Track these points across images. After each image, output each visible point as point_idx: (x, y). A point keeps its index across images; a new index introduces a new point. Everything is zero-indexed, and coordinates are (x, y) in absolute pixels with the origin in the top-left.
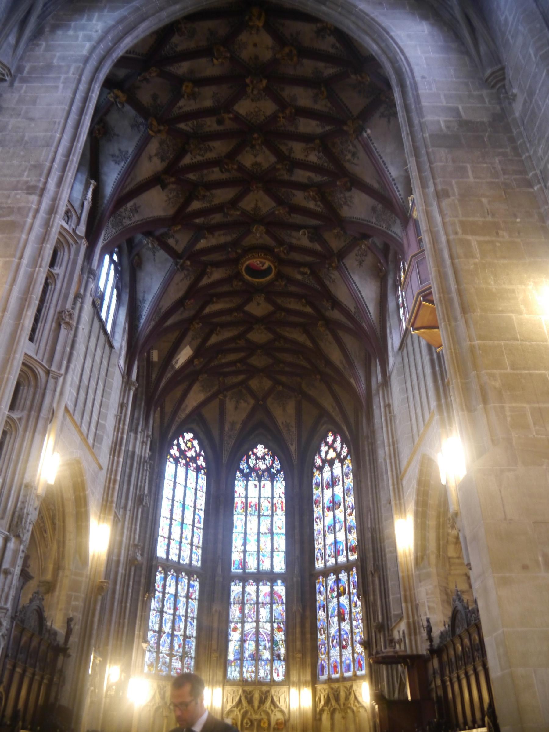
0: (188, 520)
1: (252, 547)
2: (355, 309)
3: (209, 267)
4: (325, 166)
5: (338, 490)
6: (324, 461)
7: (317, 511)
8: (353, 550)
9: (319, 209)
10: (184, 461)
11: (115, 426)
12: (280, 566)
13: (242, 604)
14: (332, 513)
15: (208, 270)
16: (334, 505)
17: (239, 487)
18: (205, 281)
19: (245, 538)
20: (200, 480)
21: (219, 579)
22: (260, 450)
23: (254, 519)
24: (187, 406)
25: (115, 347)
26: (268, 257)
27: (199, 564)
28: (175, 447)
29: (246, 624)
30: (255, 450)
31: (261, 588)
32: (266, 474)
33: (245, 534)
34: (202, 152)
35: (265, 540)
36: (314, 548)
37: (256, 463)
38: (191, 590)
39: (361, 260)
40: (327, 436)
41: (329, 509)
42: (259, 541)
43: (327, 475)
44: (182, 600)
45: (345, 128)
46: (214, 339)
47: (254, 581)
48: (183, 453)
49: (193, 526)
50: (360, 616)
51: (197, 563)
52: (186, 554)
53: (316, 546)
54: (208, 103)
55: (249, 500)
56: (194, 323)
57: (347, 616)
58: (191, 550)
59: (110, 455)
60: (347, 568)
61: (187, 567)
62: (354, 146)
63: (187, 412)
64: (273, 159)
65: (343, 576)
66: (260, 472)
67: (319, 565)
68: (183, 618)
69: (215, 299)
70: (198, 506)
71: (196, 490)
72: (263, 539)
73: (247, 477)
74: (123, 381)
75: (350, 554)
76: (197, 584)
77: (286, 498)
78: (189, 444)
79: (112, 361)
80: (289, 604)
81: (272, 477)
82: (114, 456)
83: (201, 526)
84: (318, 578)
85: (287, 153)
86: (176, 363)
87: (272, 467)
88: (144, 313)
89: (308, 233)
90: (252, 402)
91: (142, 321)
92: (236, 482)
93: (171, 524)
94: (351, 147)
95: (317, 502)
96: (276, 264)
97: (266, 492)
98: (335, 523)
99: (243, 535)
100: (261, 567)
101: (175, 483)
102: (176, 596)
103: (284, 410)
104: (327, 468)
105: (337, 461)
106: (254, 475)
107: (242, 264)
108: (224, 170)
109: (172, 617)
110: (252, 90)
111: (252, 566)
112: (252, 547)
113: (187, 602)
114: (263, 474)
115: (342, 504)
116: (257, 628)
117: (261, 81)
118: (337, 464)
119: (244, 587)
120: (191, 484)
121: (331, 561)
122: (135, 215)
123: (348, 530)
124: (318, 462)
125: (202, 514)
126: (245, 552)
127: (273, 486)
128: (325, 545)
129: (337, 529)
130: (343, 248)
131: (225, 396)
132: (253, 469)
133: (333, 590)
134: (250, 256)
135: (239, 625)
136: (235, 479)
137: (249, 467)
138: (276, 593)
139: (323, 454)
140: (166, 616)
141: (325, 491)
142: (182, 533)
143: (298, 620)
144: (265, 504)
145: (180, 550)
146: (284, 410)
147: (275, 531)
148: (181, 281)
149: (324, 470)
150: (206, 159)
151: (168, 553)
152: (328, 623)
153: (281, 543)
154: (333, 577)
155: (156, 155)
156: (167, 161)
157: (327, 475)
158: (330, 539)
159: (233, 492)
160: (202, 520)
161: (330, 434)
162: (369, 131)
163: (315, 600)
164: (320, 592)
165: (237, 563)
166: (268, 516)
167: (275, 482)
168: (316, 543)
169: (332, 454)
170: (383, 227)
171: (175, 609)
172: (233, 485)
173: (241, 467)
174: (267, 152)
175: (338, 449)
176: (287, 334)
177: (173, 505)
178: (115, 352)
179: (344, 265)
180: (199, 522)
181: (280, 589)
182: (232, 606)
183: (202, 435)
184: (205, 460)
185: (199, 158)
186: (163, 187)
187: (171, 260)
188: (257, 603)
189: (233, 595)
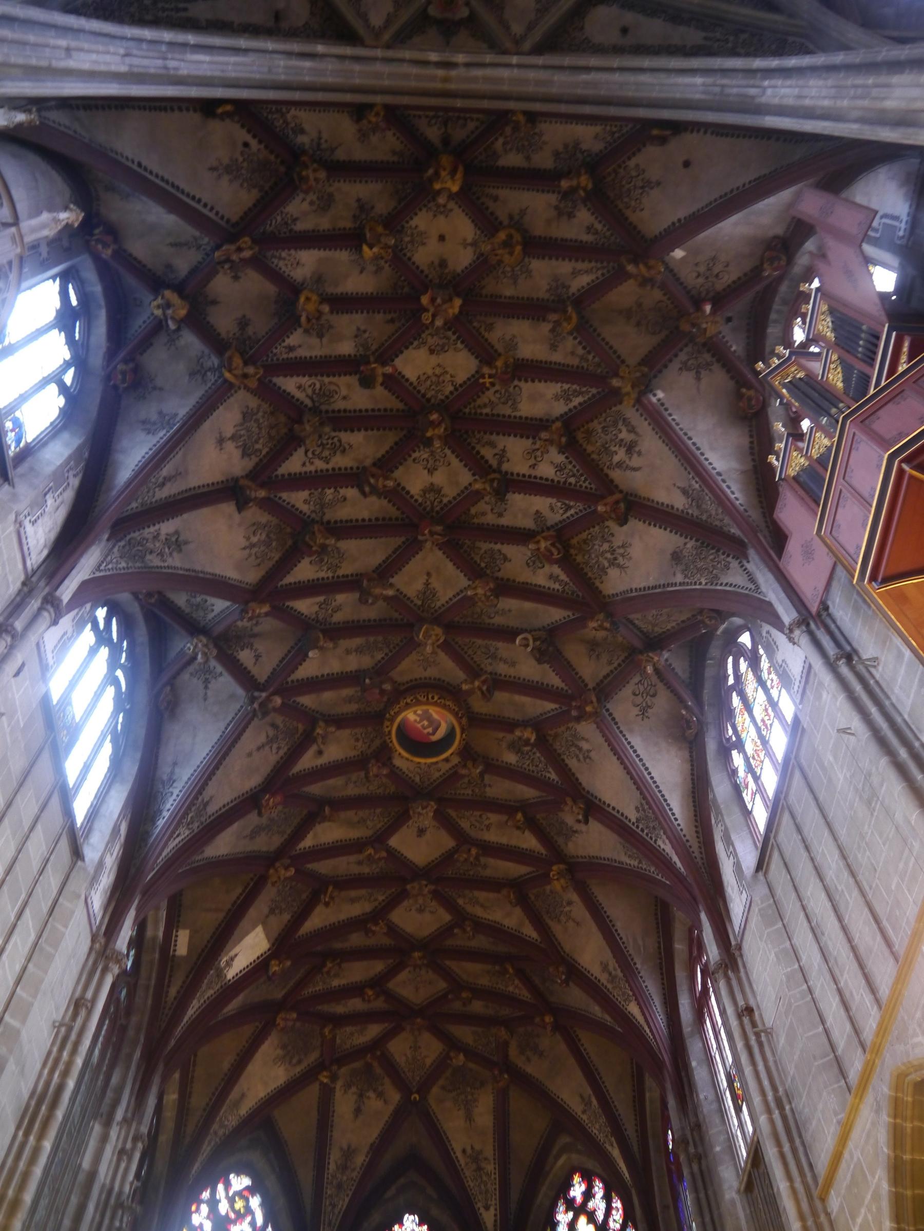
2: (638, 811)
3: (321, 724)
4: (570, 484)
9: (557, 586)
11: (49, 1053)
15: (319, 731)
18: (308, 761)
24: (243, 1096)
25: (86, 859)
26: (448, 703)
28: (204, 1208)
34: (326, 453)
39: (644, 705)
40: (569, 1185)
45: (615, 382)
46: (318, 920)
54: (346, 348)
56: (277, 864)
59: (18, 1128)
62: (632, 430)
63: (244, 1110)
64: (465, 477)
69: (327, 809)
74: (91, 949)
78: (239, 1205)
79: (71, 887)
82: (27, 1134)
85: (494, 463)
86: (229, 964)
88: (168, 806)
89: (535, 640)
90: (395, 1097)
91: (161, 823)
94: (624, 435)
96: (464, 721)
103: (469, 1118)
107: (392, 720)
108: (367, 489)
110: (434, 316)
117: (451, 300)
122: (175, 554)
130: (605, 677)
131: (334, 1078)
134: (409, 701)
146: (469, 1118)
148: (259, 749)
150: (333, 469)
155: (233, 438)
156: (255, 460)
161: (577, 1179)
162: (660, 394)
170: (700, 584)
174: (455, 462)
175: (600, 1216)
176: (479, 912)
178: (85, 869)
179: (610, 715)
183: (272, 1182)
185: (319, 465)
186: (240, 508)
187: (240, 692)
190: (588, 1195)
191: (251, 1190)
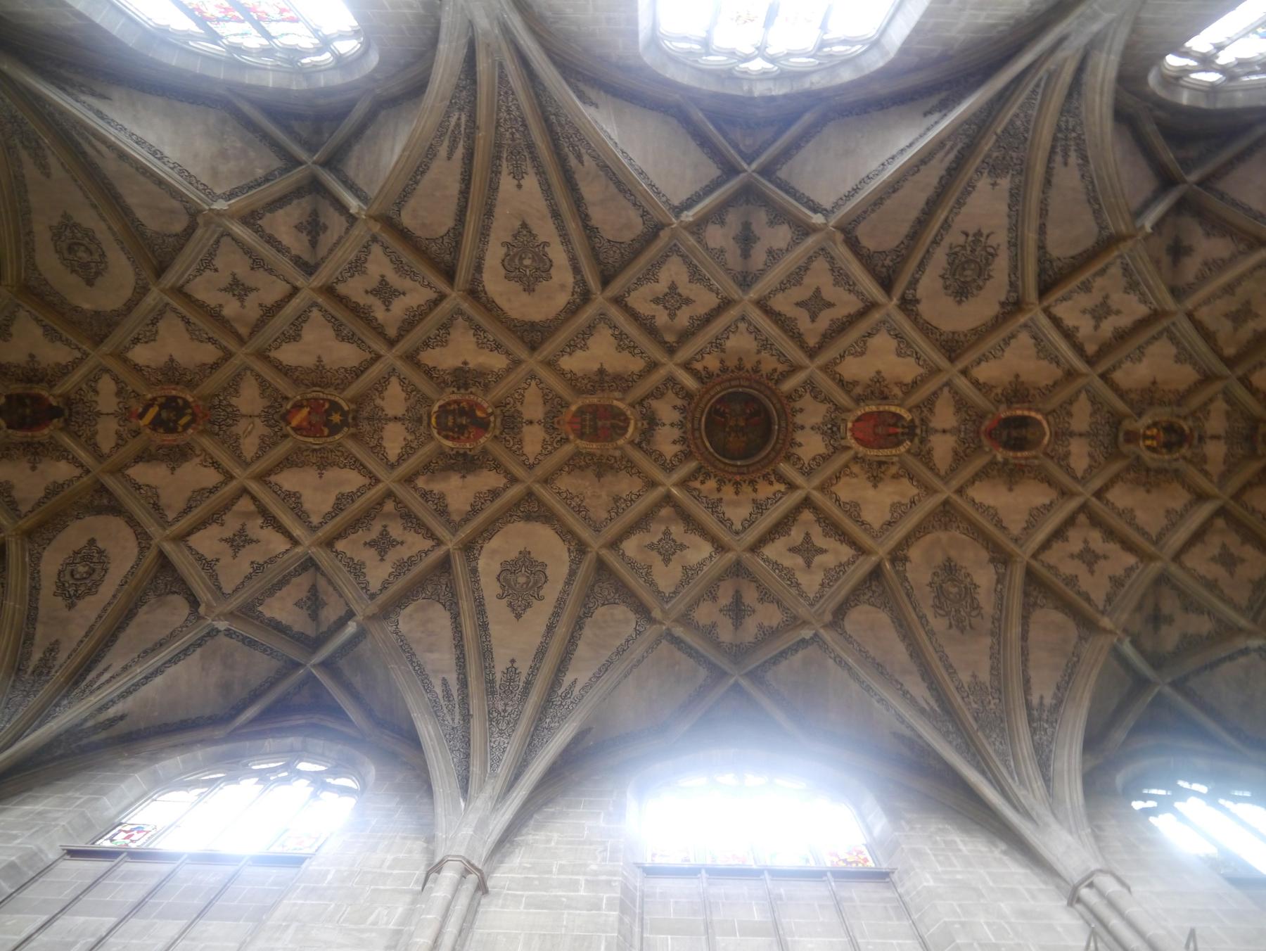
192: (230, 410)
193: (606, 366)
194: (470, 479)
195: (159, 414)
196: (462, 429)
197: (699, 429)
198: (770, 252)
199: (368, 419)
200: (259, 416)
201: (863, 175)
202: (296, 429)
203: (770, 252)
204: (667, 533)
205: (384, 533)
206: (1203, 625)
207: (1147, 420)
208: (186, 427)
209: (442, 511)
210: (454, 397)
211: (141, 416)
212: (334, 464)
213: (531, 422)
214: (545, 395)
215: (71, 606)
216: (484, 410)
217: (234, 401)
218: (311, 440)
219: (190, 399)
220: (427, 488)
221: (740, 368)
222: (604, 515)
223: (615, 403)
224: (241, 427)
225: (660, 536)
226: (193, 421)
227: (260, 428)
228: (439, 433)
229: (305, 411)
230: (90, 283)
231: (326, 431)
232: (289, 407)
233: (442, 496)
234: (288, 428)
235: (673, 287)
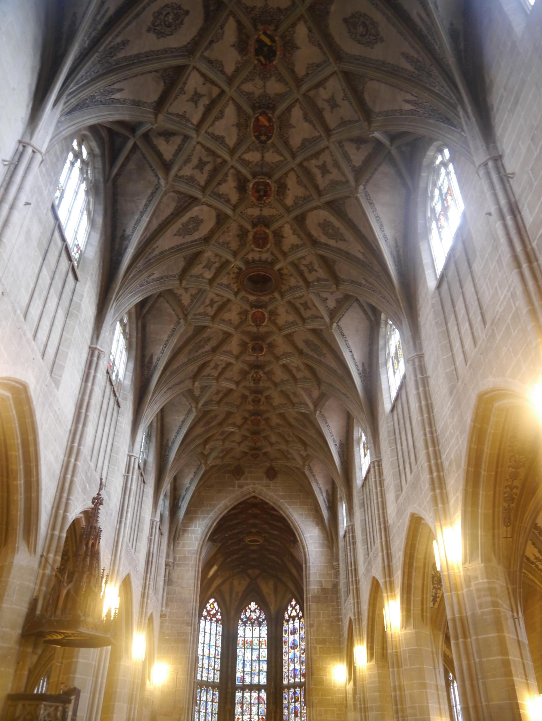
0: (212, 655)
1: (248, 669)
5: (297, 637)
6: (290, 616)
7: (285, 648)
8: (303, 675)
10: (209, 618)
12: (263, 681)
13: (242, 704)
14: (293, 651)
16: (294, 647)
17: (240, 632)
19: (244, 663)
20: (218, 629)
21: (230, 690)
22: (253, 606)
23: (249, 651)
27: (218, 681)
29: (244, 716)
30: (250, 606)
31: (252, 694)
32: (256, 622)
33: (244, 660)
35: (255, 664)
36: (283, 671)
37: (250, 615)
38: (214, 697)
40: (291, 601)
41: (291, 647)
42: (251, 665)
43: (291, 626)
44: (210, 703)
47: (249, 690)
48: (208, 612)
49: (215, 657)
50: (305, 715)
51: (217, 681)
52: (211, 676)
53: (284, 670)
55: (246, 639)
57: (299, 714)
58: (214, 672)
60: (301, 685)
61: (212, 684)
65: (298, 690)
66: (253, 621)
67: (285, 682)
68: (210, 714)
70: (218, 645)
71: (216, 634)
72: (254, 664)
73: (245, 623)
75: (302, 678)
76: (217, 693)
77: (267, 638)
78: (212, 606)
80: (268, 704)
81: (260, 624)
83: (219, 657)
84: (284, 690)
87: (259, 617)
90: (248, 580)
92: (239, 627)
93: (203, 659)
95: (285, 642)
97: (256, 634)
98: (294, 657)
99: (242, 661)
100: (253, 682)
101: (205, 632)
102: (206, 702)
104: (291, 622)
105: (297, 618)
106: (249, 622)
109: (204, 714)
111: (248, 680)
112: (248, 669)
113: (212, 704)
114: (254, 622)
115: (299, 647)
116: (250, 718)
118: (297, 621)
119: (243, 694)
120: (213, 632)
121: (292, 680)
123: (301, 663)
124: (286, 616)
125: (219, 649)
126: (244, 672)
127: (260, 630)
128: (288, 670)
129: (296, 661)
132: (249, 619)
133: (292, 698)
135: (240, 717)
136: (238, 625)
137: (246, 617)
138: (261, 697)
139: (289, 612)
140: (202, 714)
141: (290, 636)
142: (209, 663)
143: (273, 715)
144: (256, 642)
145: (208, 673)
147: (261, 659)
149: (290, 623)
151: (202, 677)
152: (289, 717)
153: (264, 667)
154: (292, 690)
157: (291, 626)
158: (291, 668)
159: (237, 634)
160: (220, 653)
161: (293, 600)
163: (283, 703)
164: (285, 698)
165: (239, 679)
166: (256, 649)
167: (261, 627)
168: (284, 668)
169: (294, 614)
171: (206, 709)
172: (237, 630)
173: (242, 617)
175: (298, 611)
177: (204, 647)
180: (218, 655)
181: (264, 695)
182: (237, 705)
184: (221, 615)
188: (251, 703)
189: (237, 698)
190: (296, 605)
191: (214, 602)
192: (268, 75)
193: (285, 239)
194: (235, 190)
195: (266, 45)
196: (258, 191)
197: (258, 271)
198: (326, 299)
199: (255, 444)
200: (265, 92)
201: (348, 339)
202: (257, 119)
203: (326, 299)
204: (215, 263)
205: (206, 163)
206: (197, 393)
207: (262, 375)
208: (259, 60)
209: (219, 184)
210: (273, 188)
211: (265, 33)
212: (239, 130)
213: (261, 210)
214: (273, 216)
215: (149, 30)
216: (266, 199)
217: (273, 79)
218: (252, 125)
219: (274, 63)
220: (230, 175)
221: (282, 283)
222: (221, 241)
223: (269, 245)
224: (259, 82)
225: (213, 261)
226: (262, 64)
227: (258, 92)
228: (256, 182)
229: (267, 124)
230: (345, 20)
231: (256, 134)
232: (269, 115)
233: (225, 181)
234: (258, 114)
235: (316, 271)
